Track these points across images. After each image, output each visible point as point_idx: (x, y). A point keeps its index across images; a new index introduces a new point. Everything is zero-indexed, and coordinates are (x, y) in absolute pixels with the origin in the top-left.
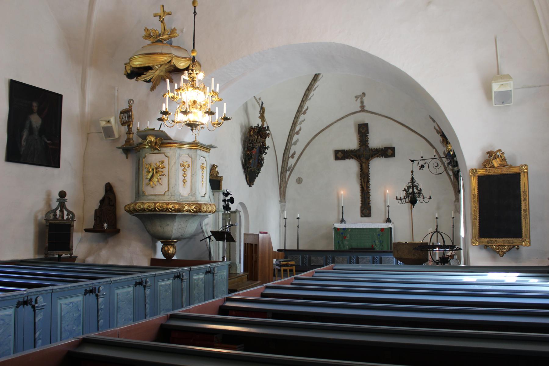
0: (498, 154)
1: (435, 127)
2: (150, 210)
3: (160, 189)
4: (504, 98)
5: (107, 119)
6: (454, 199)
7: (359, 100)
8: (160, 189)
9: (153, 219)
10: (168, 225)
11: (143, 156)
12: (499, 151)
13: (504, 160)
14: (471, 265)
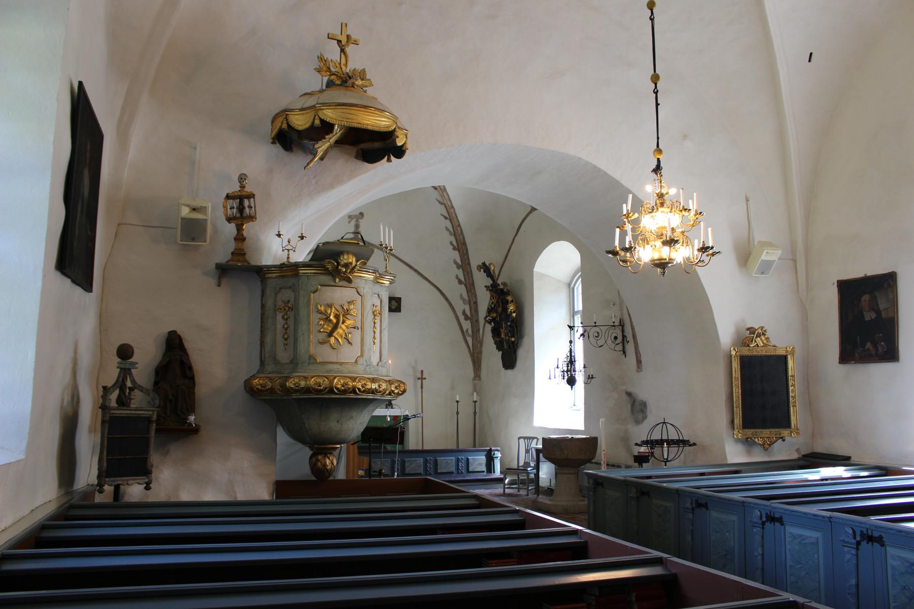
0: (760, 331)
1: (457, 277)
2: (319, 392)
3: (348, 354)
4: (766, 267)
5: (197, 203)
6: (472, 375)
7: (353, 222)
8: (348, 354)
9: (294, 404)
10: (352, 418)
11: (313, 289)
12: (762, 328)
13: (767, 339)
14: (729, 462)
